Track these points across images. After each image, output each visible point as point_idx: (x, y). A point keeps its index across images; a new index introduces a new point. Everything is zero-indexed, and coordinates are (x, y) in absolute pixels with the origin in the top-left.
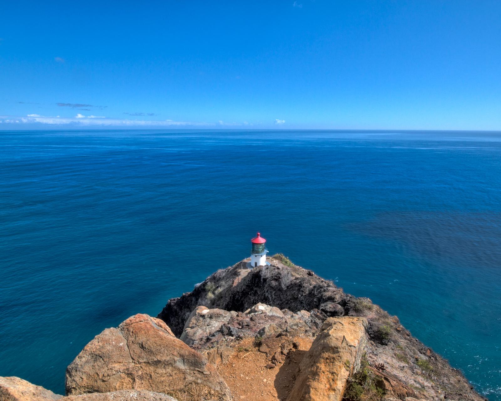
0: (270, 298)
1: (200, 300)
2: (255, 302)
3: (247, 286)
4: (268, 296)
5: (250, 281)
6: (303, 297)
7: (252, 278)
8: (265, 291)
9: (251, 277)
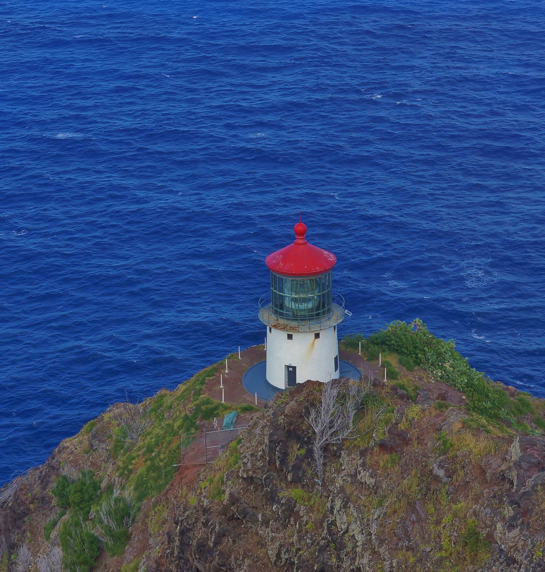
0: (360, 538)
1: (24, 551)
2: (284, 556)
3: (250, 480)
4: (347, 531)
5: (262, 457)
6: (517, 531)
7: (272, 450)
8: (332, 508)
9: (266, 441)
